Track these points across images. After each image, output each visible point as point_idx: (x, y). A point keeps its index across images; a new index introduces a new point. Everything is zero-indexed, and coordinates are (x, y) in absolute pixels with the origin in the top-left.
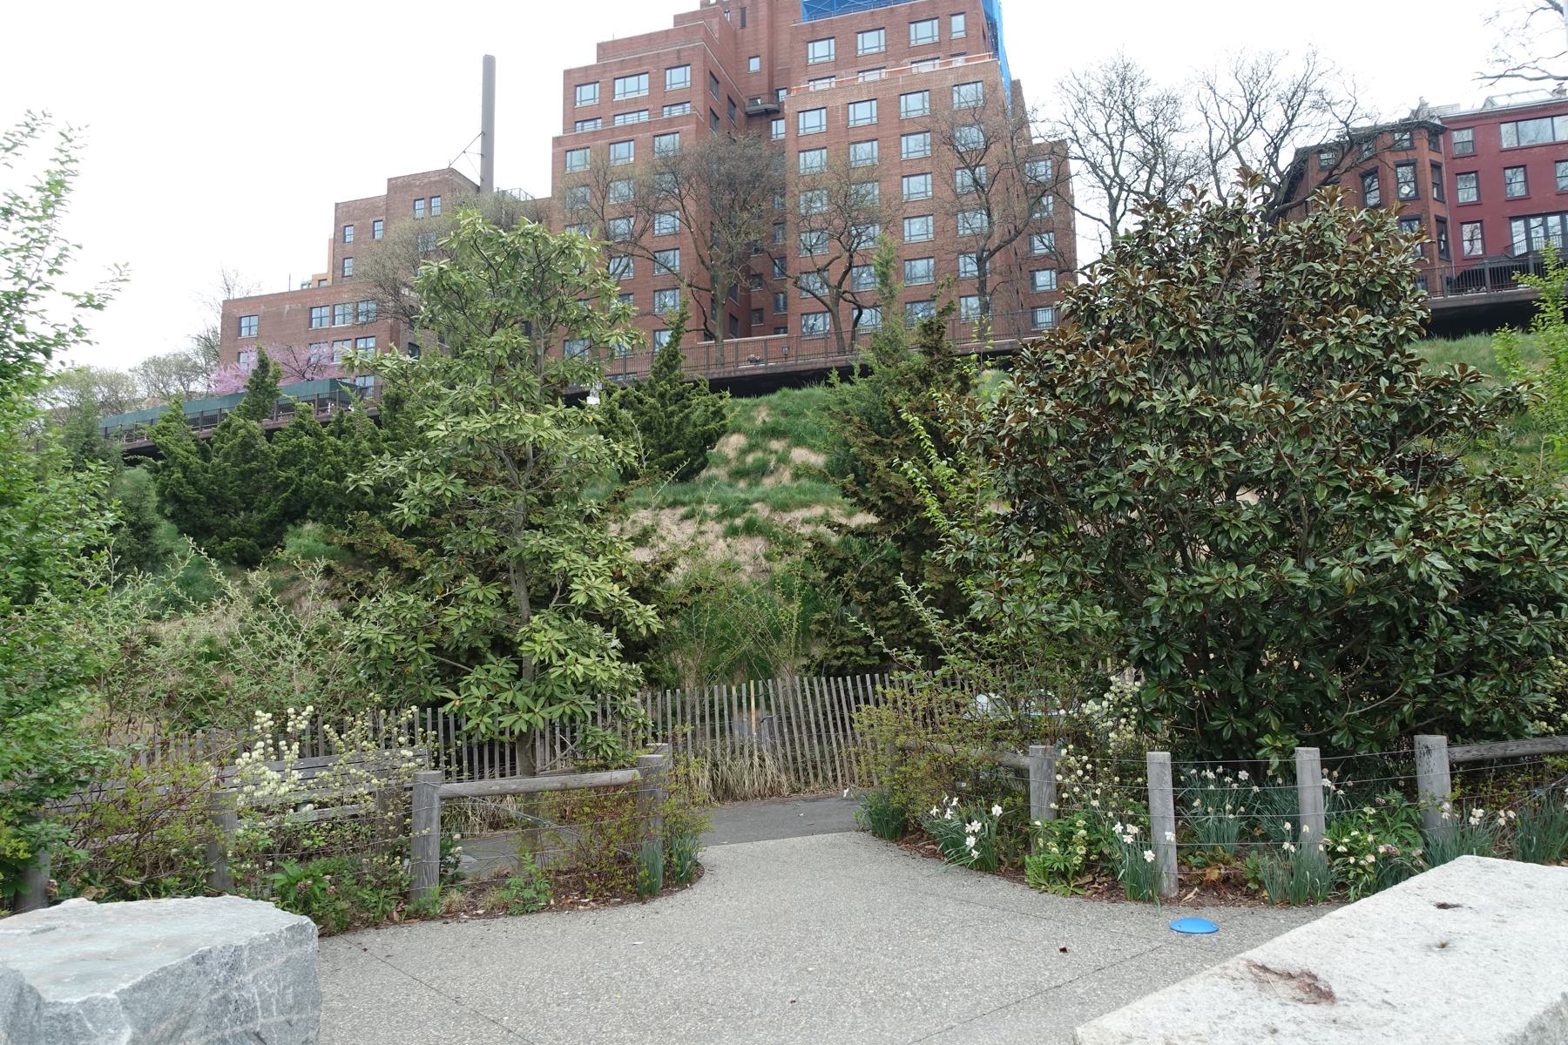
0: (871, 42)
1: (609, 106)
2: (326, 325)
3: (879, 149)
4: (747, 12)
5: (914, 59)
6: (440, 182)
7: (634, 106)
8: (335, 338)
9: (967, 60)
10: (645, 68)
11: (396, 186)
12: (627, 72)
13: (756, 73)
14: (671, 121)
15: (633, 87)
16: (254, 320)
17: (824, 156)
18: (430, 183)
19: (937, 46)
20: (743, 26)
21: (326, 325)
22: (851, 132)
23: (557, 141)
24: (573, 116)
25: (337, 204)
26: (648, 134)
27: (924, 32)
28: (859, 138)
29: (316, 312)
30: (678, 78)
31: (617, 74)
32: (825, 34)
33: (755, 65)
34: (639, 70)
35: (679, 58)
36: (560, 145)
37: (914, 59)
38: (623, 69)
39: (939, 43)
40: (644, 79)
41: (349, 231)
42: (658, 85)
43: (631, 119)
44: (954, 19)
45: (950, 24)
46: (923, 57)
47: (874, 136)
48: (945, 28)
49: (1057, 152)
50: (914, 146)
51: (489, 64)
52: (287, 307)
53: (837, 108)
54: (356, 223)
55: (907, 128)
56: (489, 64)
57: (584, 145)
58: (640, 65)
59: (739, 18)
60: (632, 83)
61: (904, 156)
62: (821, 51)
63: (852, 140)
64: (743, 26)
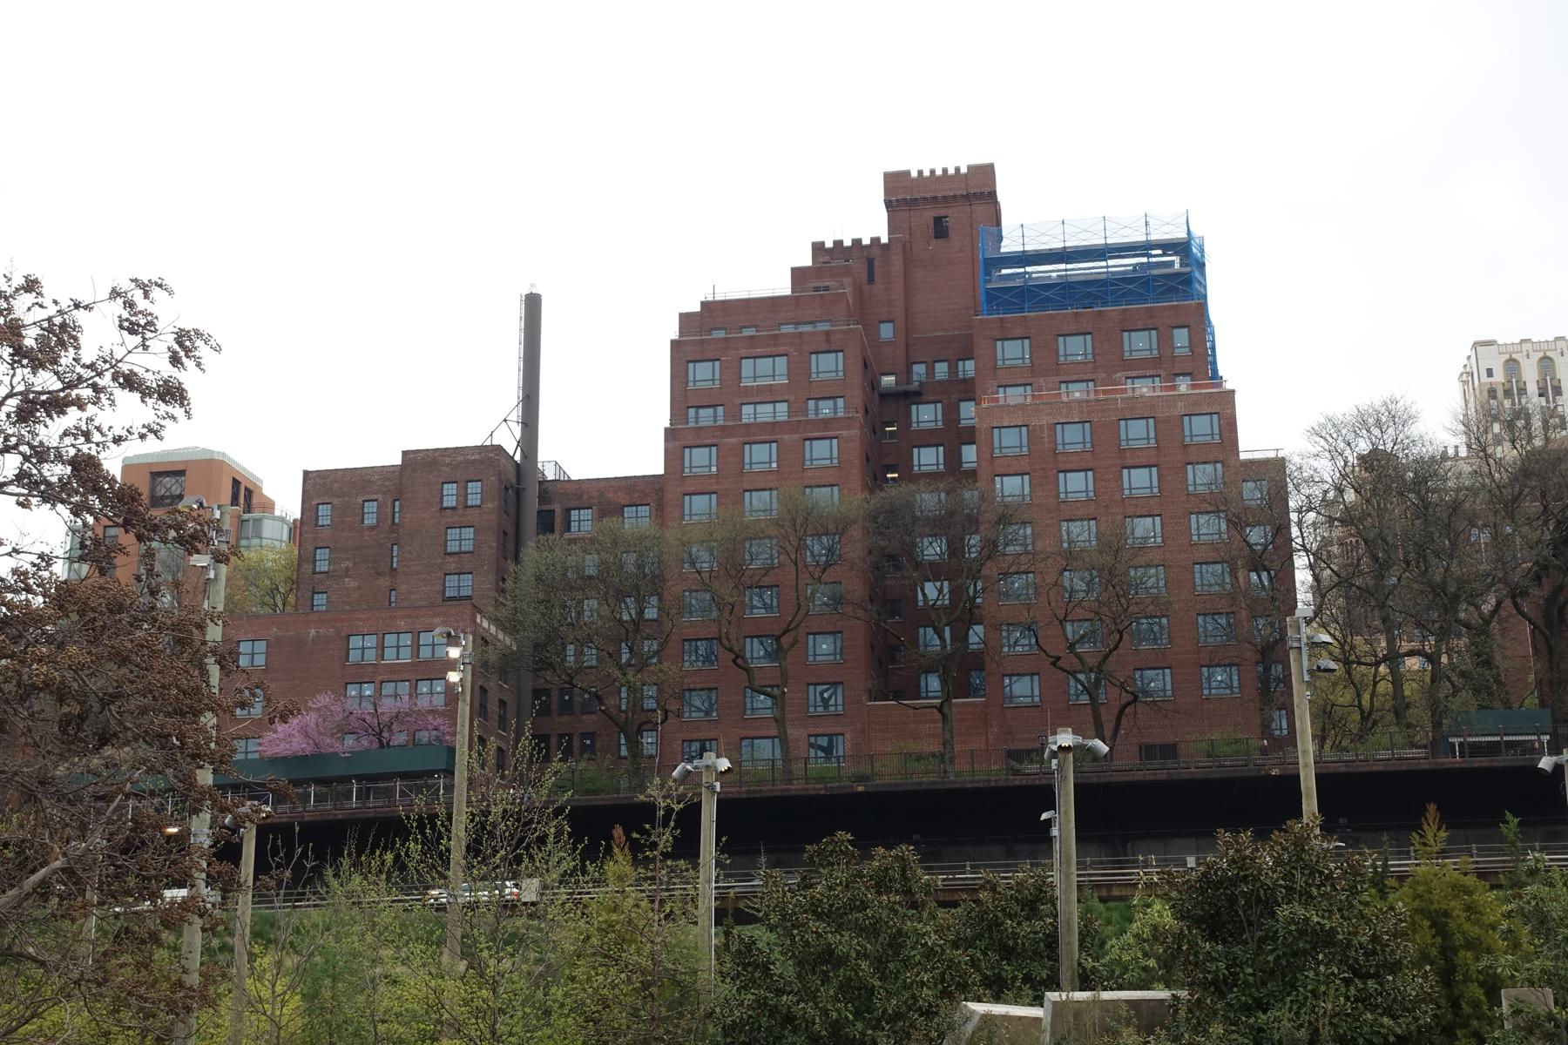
0: (1075, 348)
1: (731, 394)
2: (371, 656)
3: (1162, 524)
4: (877, 264)
5: (1130, 374)
6: (481, 462)
7: (767, 395)
8: (385, 677)
9: (1194, 387)
10: (781, 349)
11: (416, 461)
12: (759, 351)
13: (889, 343)
14: (826, 423)
15: (768, 371)
16: (261, 646)
17: (1094, 529)
18: (466, 462)
19: (1157, 361)
20: (871, 280)
21: (371, 656)
22: (1060, 458)
23: (670, 434)
24: (683, 398)
25: (306, 473)
26: (796, 436)
27: (1140, 343)
28: (1069, 466)
29: (355, 642)
30: (827, 366)
31: (743, 352)
32: (1018, 332)
33: (887, 331)
34: (774, 350)
35: (828, 341)
36: (675, 439)
37: (1130, 374)
38: (752, 347)
39: (1160, 358)
40: (781, 363)
41: (324, 510)
42: (799, 371)
43: (765, 413)
44: (1175, 331)
45: (1172, 337)
46: (1140, 373)
47: (1090, 465)
48: (1165, 341)
49: (1273, 472)
50: (1140, 480)
51: (533, 305)
52: (313, 632)
53: (1042, 427)
54: (336, 501)
55: (1129, 460)
56: (533, 305)
57: (709, 442)
58: (775, 345)
59: (865, 271)
60: (765, 365)
61: (1127, 492)
62: (1013, 352)
63: (1062, 466)
64: (871, 280)
